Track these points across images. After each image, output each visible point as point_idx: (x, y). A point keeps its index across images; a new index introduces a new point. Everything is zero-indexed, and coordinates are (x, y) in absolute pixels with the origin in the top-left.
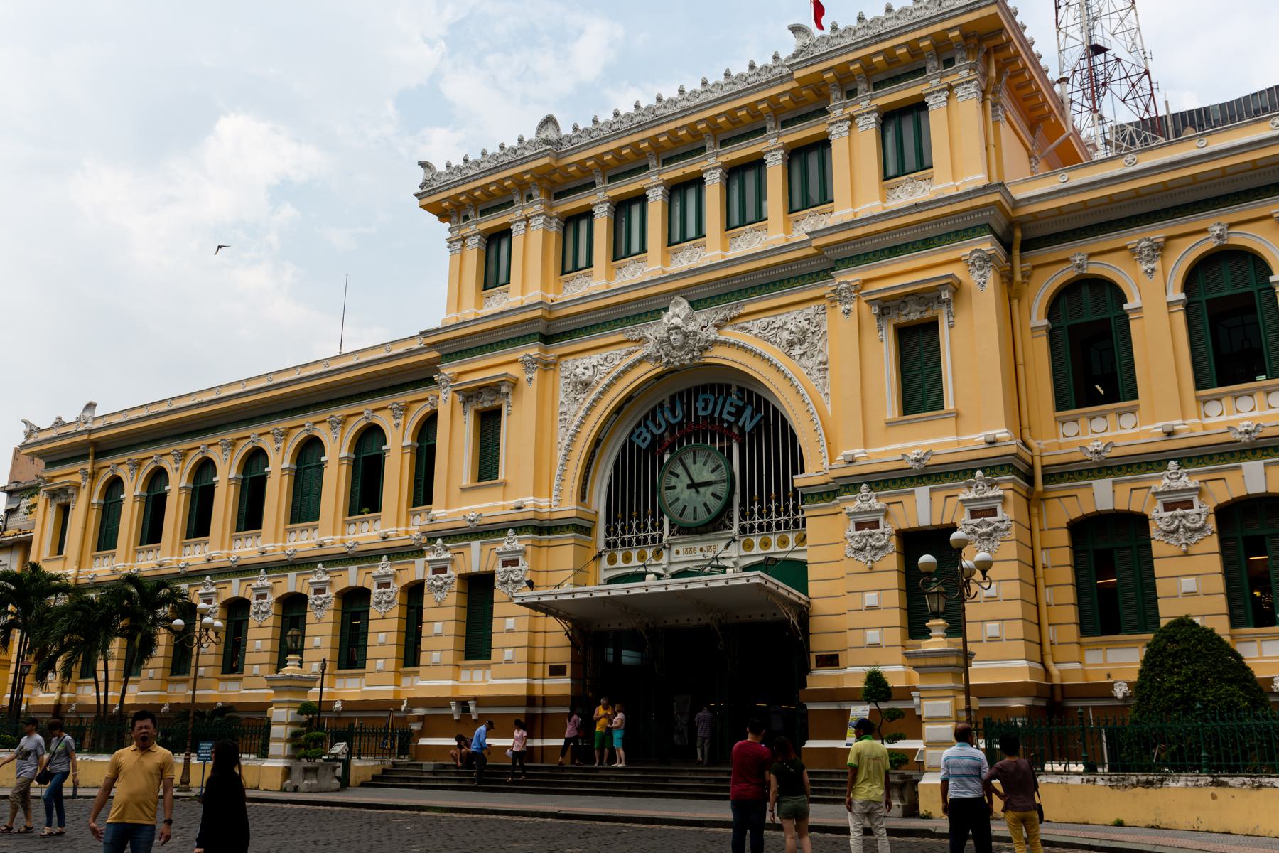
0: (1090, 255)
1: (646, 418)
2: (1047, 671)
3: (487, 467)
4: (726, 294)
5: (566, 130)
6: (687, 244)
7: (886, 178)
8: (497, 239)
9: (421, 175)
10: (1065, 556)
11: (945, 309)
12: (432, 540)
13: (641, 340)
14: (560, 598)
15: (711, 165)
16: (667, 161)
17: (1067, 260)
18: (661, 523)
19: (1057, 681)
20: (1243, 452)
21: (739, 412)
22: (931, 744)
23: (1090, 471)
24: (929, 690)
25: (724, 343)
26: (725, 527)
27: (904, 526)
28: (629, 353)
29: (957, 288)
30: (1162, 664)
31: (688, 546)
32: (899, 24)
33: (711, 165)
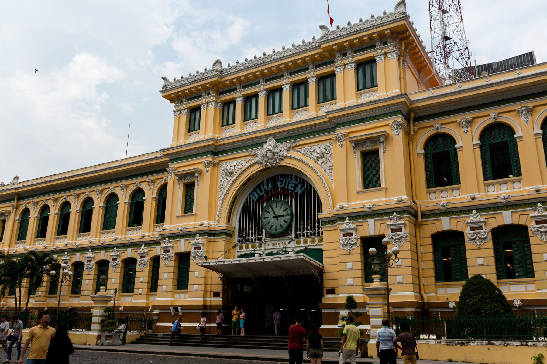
0: (442, 124)
1: (256, 188)
2: (422, 296)
3: (188, 207)
4: (291, 137)
5: (225, 66)
6: (275, 115)
7: (358, 90)
8: (195, 111)
9: (163, 83)
10: (430, 249)
11: (382, 145)
12: (164, 238)
13: (255, 155)
14: (218, 263)
15: (286, 83)
16: (267, 80)
17: (432, 126)
18: (262, 232)
19: (426, 301)
20: (503, 207)
21: (295, 186)
22: (373, 327)
23: (440, 213)
24: (373, 304)
25: (290, 157)
26: (289, 235)
27: (363, 235)
28: (250, 161)
29: (387, 137)
30: (469, 294)
32: (365, 27)
33: (286, 83)
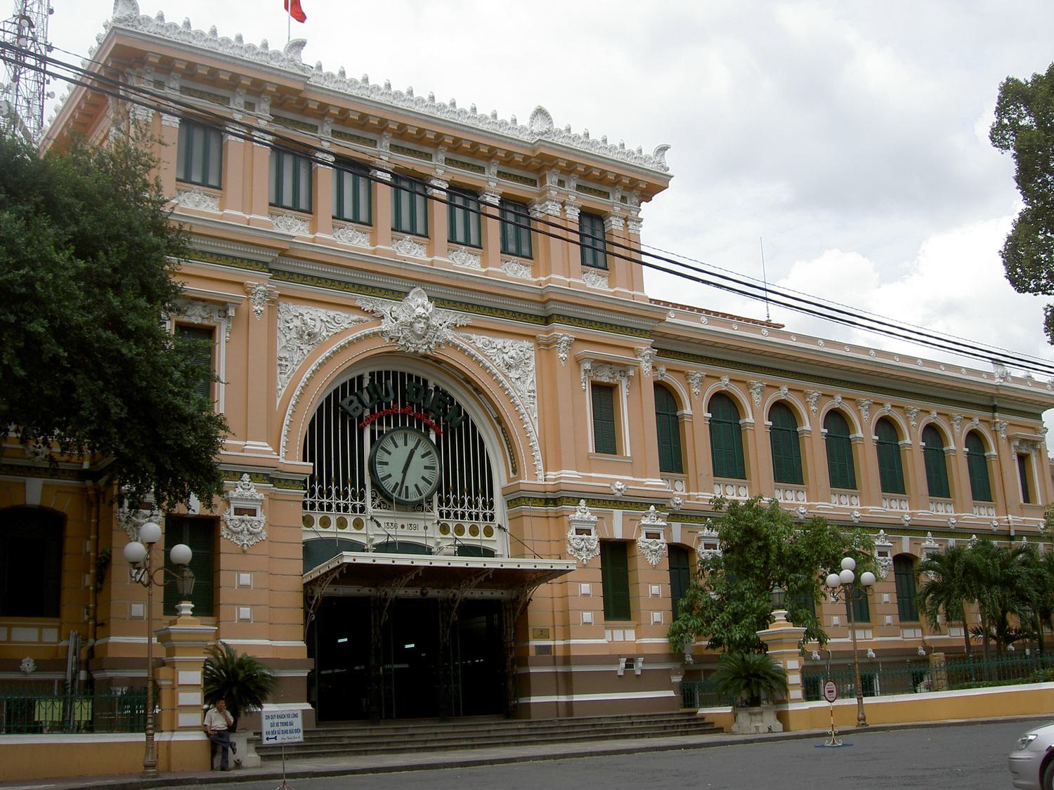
25: (456, 346)
31: (391, 521)
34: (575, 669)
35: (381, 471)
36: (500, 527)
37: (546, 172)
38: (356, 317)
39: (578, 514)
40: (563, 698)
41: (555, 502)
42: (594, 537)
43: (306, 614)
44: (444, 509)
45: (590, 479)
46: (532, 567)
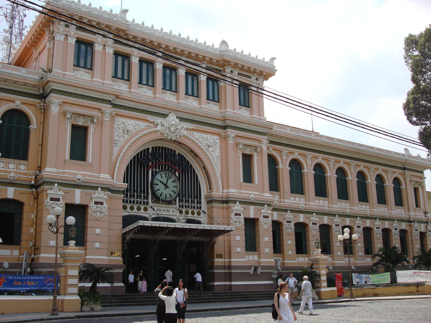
25: (187, 137)
31: (159, 208)
34: (233, 271)
35: (156, 188)
36: (203, 212)
37: (226, 67)
38: (146, 124)
39: (236, 207)
40: (228, 283)
41: (227, 202)
42: (242, 217)
43: (123, 246)
44: (181, 204)
45: (241, 193)
46: (216, 229)
